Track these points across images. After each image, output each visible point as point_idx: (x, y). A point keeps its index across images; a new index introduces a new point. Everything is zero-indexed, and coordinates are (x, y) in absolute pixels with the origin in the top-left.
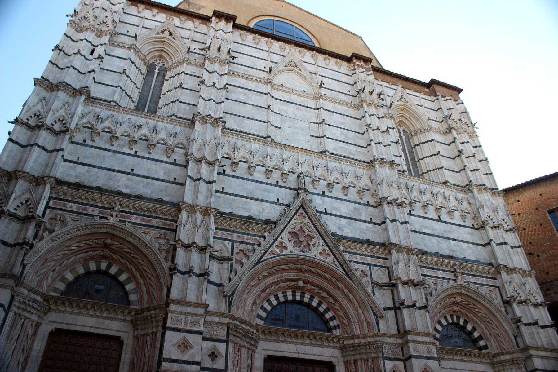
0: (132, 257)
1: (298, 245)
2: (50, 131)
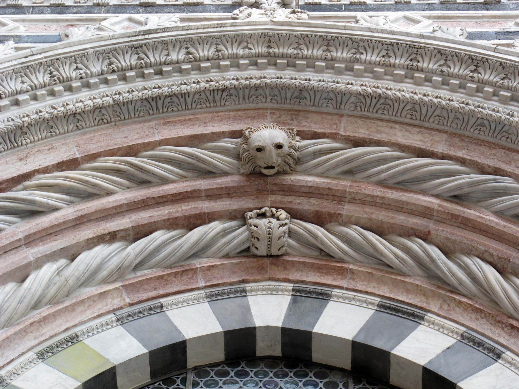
0: (457, 198)
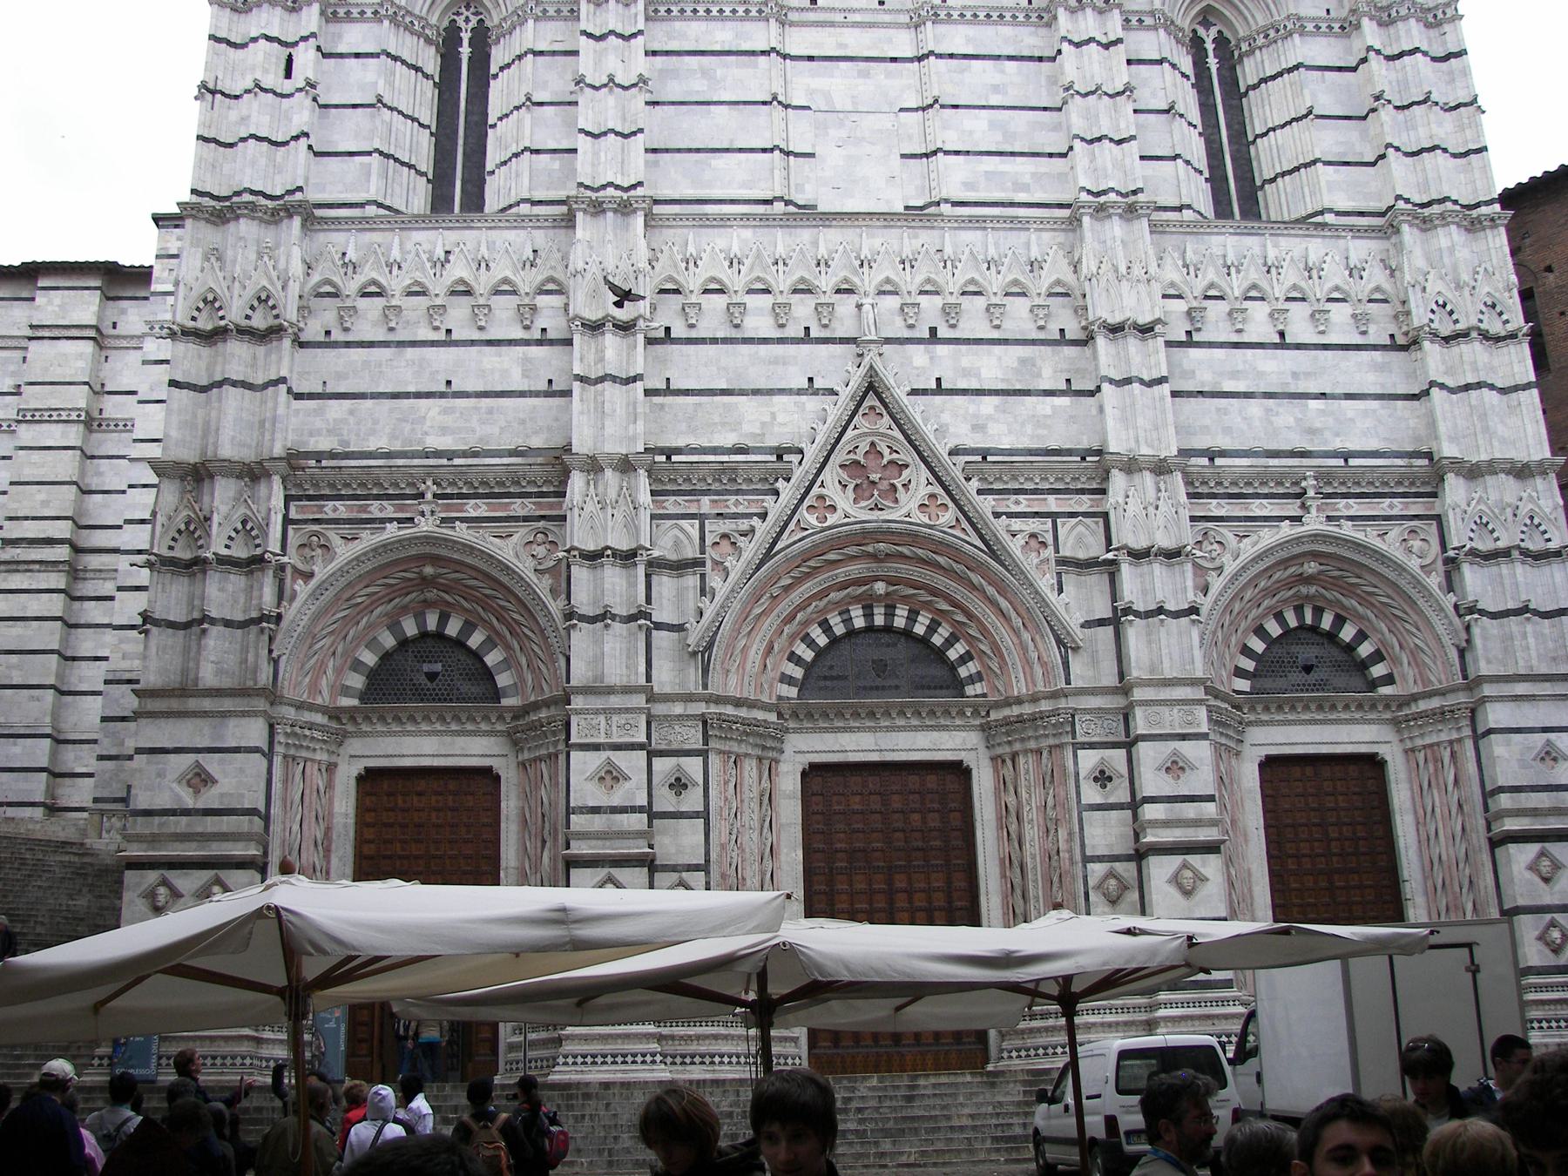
1: (867, 494)
2: (247, 338)
